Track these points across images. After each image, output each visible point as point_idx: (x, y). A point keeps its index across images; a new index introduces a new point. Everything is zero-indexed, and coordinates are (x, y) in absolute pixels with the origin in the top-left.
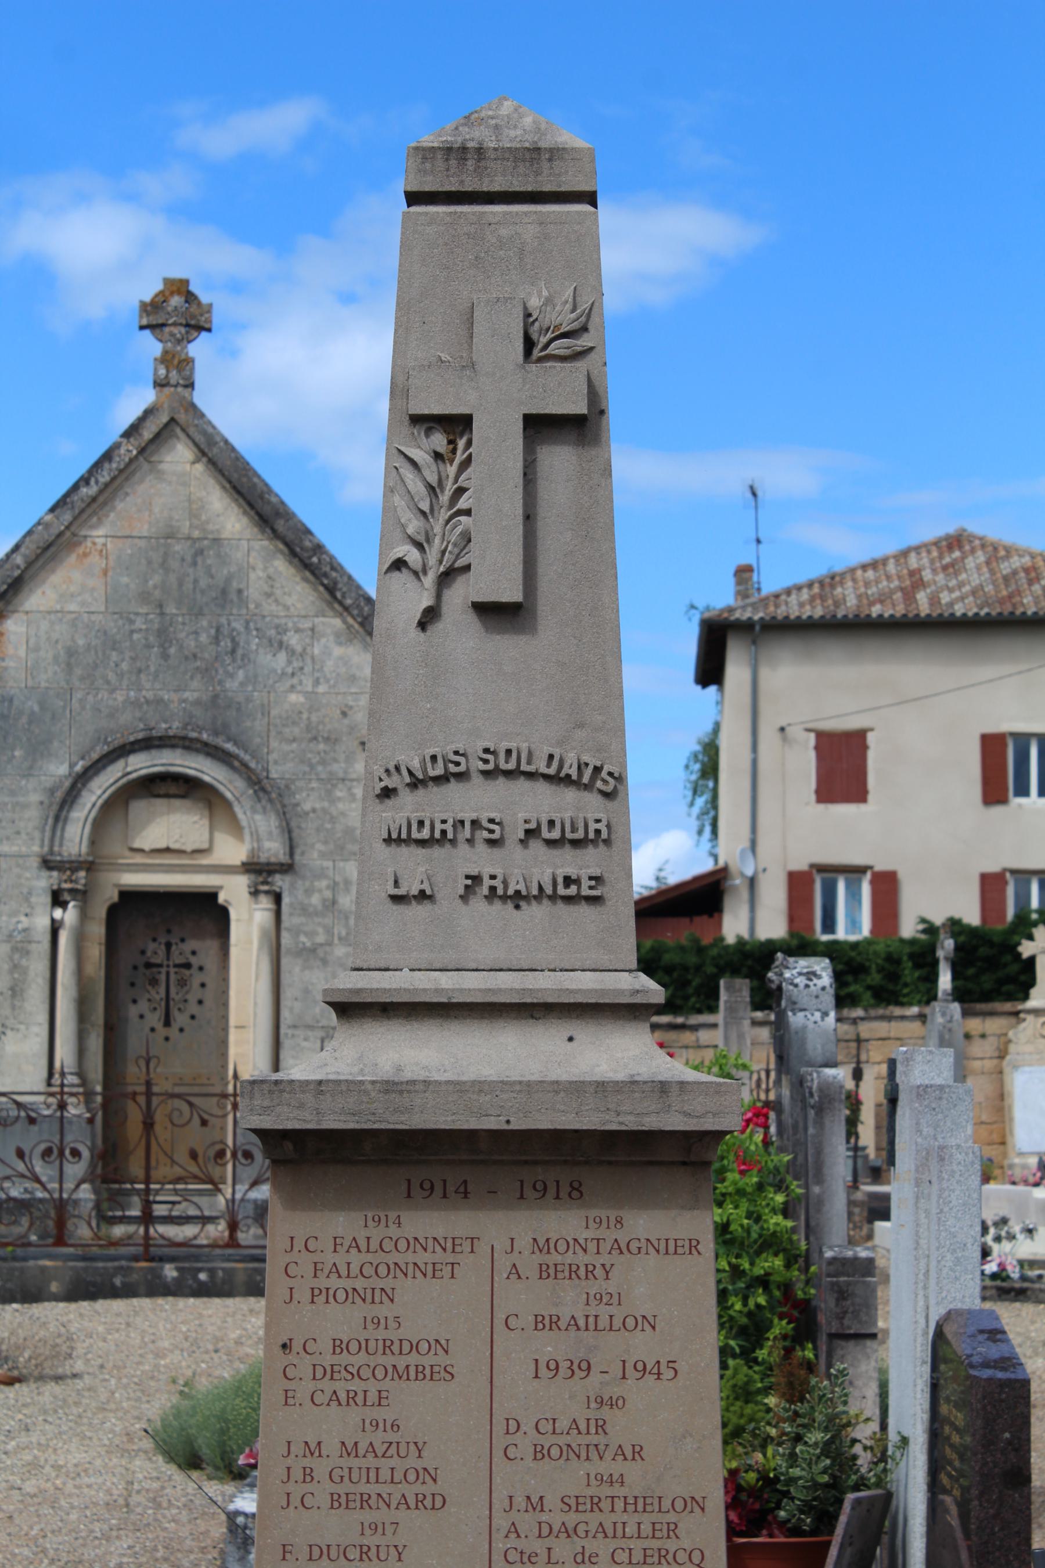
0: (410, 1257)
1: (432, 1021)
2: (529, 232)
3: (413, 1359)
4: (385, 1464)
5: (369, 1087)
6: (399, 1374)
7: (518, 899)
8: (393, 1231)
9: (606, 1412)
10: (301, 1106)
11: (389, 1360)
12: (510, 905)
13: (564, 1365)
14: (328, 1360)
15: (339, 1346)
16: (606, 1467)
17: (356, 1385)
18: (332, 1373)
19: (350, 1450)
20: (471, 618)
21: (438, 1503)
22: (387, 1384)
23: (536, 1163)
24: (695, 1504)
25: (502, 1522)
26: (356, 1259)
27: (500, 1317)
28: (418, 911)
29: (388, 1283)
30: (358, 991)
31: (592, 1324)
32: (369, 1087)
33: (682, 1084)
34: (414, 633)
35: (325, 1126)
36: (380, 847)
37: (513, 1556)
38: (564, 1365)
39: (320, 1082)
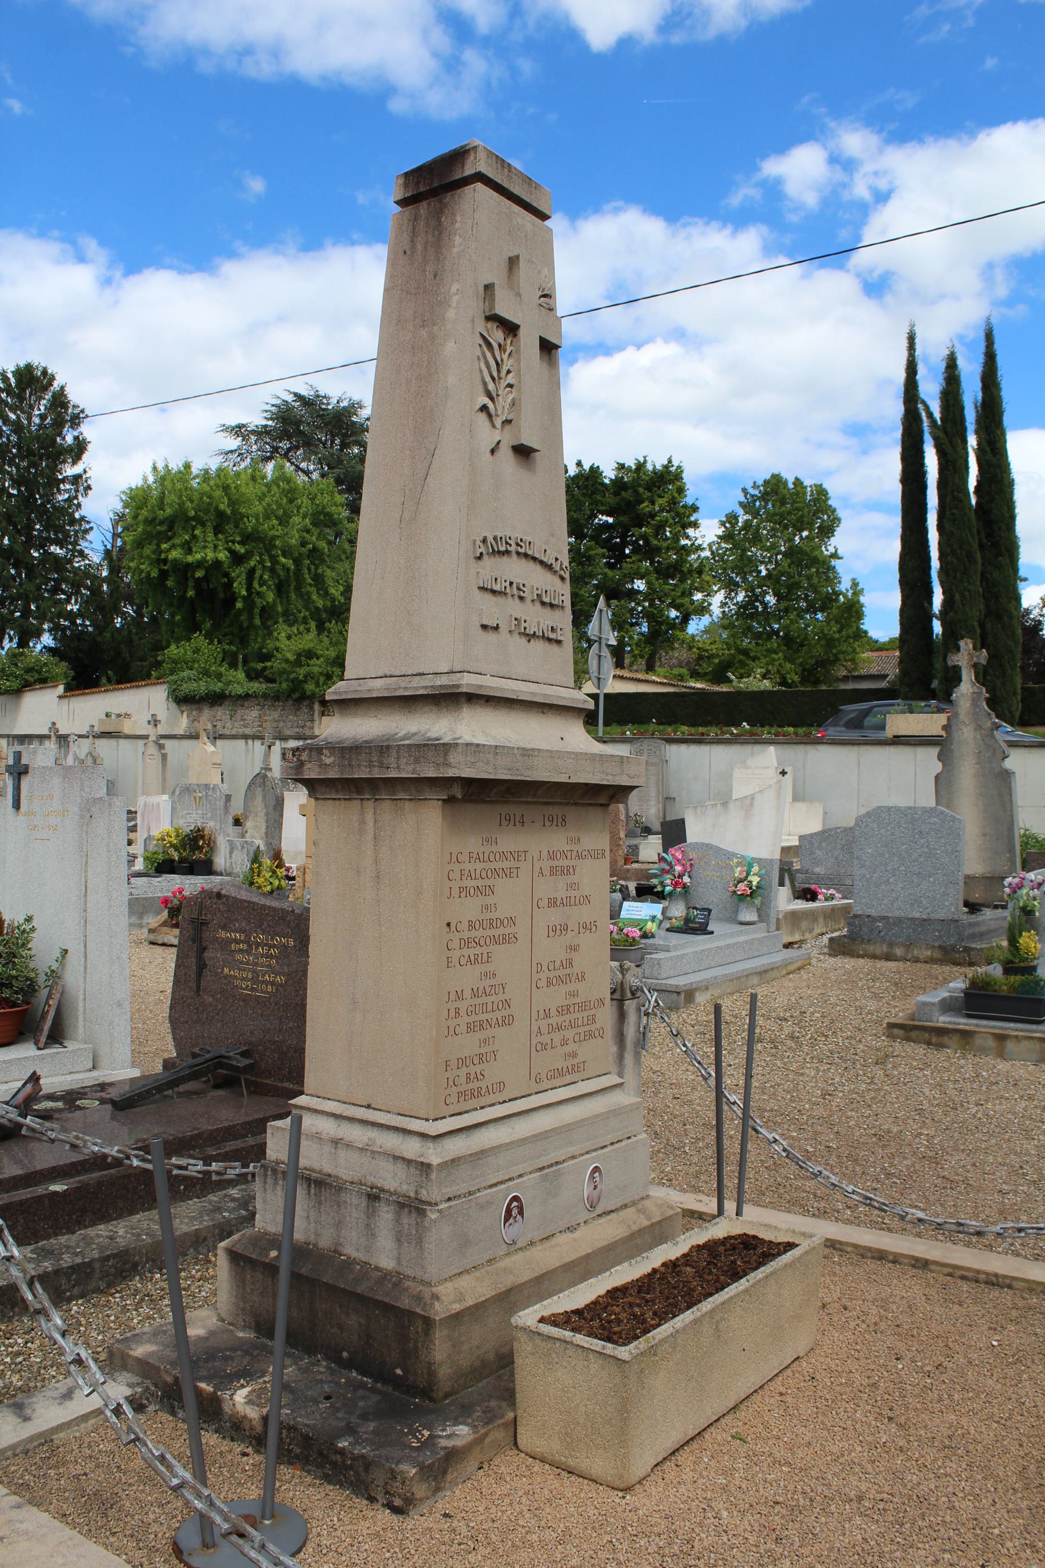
0: (501, 865)
1: (426, 709)
2: (529, 227)
3: (501, 931)
4: (489, 999)
5: (516, 751)
6: (495, 941)
7: (530, 637)
8: (494, 848)
9: (573, 955)
10: (488, 763)
11: (490, 932)
12: (524, 640)
13: (558, 927)
14: (466, 935)
15: (471, 925)
16: (572, 987)
17: (478, 950)
18: (466, 943)
19: (475, 994)
20: (510, 453)
21: (507, 1022)
22: (491, 948)
23: (554, 803)
24: (601, 1001)
25: (535, 1029)
26: (479, 866)
27: (535, 900)
28: (492, 636)
29: (489, 882)
30: (481, 687)
31: (566, 903)
32: (516, 751)
33: (601, 756)
34: (488, 454)
35: (497, 777)
36: (476, 591)
37: (539, 1047)
38: (558, 927)
39: (496, 747)
